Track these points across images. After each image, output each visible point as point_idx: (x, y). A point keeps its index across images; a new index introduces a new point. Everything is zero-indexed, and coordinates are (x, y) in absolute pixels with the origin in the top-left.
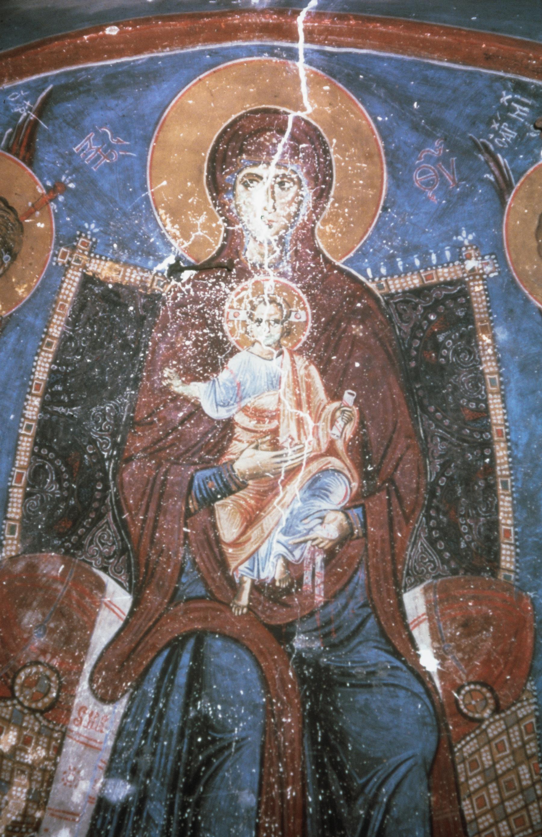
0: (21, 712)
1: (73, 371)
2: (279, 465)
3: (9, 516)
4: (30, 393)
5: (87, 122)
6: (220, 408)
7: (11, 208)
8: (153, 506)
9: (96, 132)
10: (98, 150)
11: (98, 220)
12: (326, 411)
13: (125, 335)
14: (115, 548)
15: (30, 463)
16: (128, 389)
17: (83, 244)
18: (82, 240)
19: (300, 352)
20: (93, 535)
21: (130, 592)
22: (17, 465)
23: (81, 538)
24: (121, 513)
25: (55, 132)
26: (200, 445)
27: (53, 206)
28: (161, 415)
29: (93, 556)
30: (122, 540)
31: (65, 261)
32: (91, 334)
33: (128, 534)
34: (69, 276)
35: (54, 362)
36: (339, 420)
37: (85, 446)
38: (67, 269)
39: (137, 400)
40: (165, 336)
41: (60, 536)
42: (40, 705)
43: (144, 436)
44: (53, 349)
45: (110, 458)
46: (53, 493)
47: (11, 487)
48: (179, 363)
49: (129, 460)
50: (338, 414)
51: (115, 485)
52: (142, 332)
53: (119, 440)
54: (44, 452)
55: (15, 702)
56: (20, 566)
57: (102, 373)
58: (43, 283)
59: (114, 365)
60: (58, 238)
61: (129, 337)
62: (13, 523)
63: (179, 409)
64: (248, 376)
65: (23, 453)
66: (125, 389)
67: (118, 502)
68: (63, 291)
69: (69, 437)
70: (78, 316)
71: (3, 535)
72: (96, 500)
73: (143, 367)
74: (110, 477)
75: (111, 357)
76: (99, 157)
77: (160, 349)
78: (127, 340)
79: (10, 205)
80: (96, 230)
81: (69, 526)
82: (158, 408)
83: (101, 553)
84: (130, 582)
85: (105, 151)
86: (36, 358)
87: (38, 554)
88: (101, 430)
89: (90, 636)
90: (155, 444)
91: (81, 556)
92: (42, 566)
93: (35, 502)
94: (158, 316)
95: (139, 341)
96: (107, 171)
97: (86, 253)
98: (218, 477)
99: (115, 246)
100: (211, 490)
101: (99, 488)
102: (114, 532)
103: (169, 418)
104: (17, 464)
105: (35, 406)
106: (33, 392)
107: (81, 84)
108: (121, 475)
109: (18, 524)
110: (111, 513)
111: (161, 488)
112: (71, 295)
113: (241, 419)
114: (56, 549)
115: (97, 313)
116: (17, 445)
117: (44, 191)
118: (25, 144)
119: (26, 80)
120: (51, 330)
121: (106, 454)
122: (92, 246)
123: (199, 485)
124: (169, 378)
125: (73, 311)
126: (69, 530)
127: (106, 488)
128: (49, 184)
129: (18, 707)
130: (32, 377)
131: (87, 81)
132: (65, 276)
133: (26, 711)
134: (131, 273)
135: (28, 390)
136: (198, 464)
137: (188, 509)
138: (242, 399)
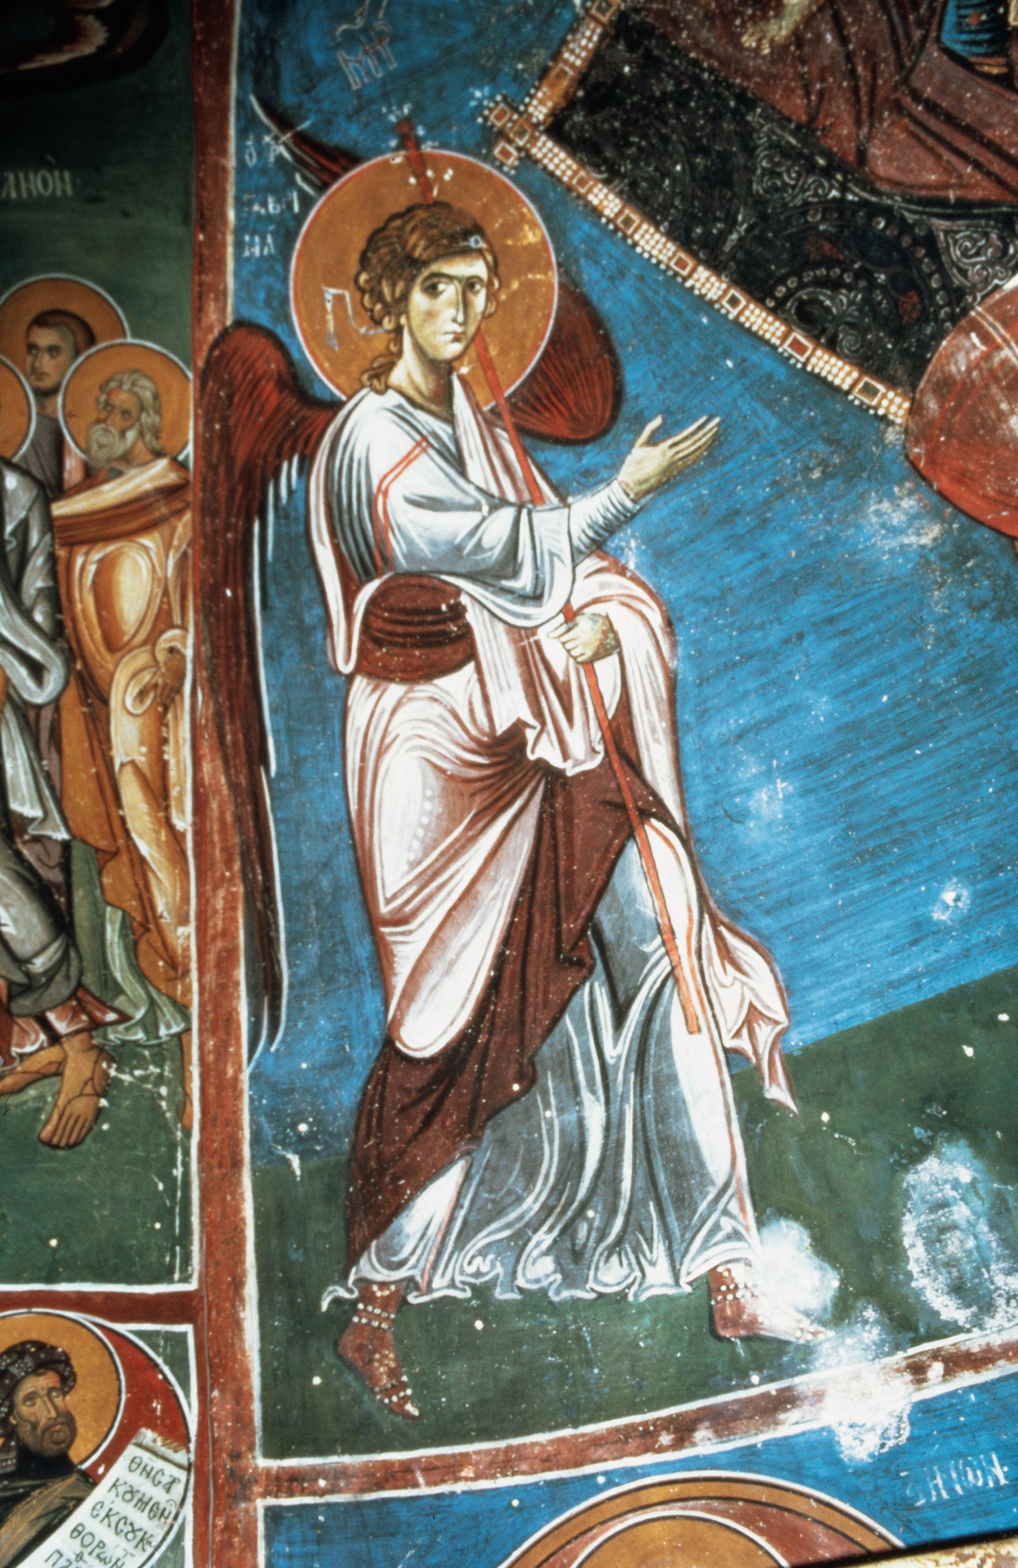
1: (684, 199)
3: (845, 387)
4: (685, 279)
5: (319, 58)
7: (410, 210)
8: (963, 143)
9: (339, 46)
10: (366, 52)
13: (664, 93)
14: (994, 236)
15: (785, 321)
16: (749, 118)
17: (498, 117)
18: (492, 118)
20: (954, 264)
22: (778, 342)
23: (946, 285)
24: (943, 203)
25: (320, 111)
26: (896, 19)
27: (427, 148)
28: (816, 73)
29: (986, 281)
30: (988, 217)
31: (515, 153)
32: (640, 149)
33: (985, 203)
34: (539, 155)
35: (657, 225)
37: (806, 222)
38: (529, 156)
39: (773, 108)
40: (688, 26)
41: (924, 318)
43: (837, 117)
44: (636, 218)
45: (844, 189)
46: (851, 303)
47: (805, 365)
48: (741, 14)
49: (862, 156)
51: (890, 196)
52: (671, 64)
53: (821, 162)
54: (781, 291)
56: (932, 405)
57: (706, 151)
58: (535, 198)
59: (702, 128)
60: (478, 155)
61: (670, 88)
62: (861, 385)
63: (819, 38)
65: (766, 326)
66: (748, 123)
67: (923, 202)
68: (558, 173)
69: (779, 243)
70: (605, 161)
71: (869, 407)
72: (898, 238)
73: (726, 80)
74: (874, 199)
75: (690, 129)
76: (378, 54)
77: (707, 41)
78: (673, 93)
79: (403, 209)
80: (487, 90)
81: (915, 299)
82: (802, 76)
83: (990, 263)
85: (370, 40)
86: (639, 250)
87: (930, 368)
88: (794, 187)
90: (858, 101)
92: (953, 368)
93: (847, 339)
94: (653, 28)
95: (683, 74)
96: (401, 46)
97: (515, 117)
99: (520, 66)
100: (983, 23)
101: (882, 225)
102: (968, 227)
103: (827, 62)
104: (776, 341)
105: (708, 280)
106: (685, 273)
107: (260, 50)
109: (866, 379)
110: (935, 221)
111: (937, 116)
112: (569, 162)
114: (939, 335)
115: (614, 130)
116: (749, 330)
117: (402, 153)
118: (325, 163)
119: (232, 132)
120: (607, 212)
121: (834, 193)
122: (509, 105)
123: (965, 43)
124: (759, 41)
125: (596, 167)
126: (922, 301)
127: (887, 212)
128: (393, 143)
130: (663, 267)
131: (259, 40)
132: (537, 162)
134: (572, 52)
136: (928, 32)
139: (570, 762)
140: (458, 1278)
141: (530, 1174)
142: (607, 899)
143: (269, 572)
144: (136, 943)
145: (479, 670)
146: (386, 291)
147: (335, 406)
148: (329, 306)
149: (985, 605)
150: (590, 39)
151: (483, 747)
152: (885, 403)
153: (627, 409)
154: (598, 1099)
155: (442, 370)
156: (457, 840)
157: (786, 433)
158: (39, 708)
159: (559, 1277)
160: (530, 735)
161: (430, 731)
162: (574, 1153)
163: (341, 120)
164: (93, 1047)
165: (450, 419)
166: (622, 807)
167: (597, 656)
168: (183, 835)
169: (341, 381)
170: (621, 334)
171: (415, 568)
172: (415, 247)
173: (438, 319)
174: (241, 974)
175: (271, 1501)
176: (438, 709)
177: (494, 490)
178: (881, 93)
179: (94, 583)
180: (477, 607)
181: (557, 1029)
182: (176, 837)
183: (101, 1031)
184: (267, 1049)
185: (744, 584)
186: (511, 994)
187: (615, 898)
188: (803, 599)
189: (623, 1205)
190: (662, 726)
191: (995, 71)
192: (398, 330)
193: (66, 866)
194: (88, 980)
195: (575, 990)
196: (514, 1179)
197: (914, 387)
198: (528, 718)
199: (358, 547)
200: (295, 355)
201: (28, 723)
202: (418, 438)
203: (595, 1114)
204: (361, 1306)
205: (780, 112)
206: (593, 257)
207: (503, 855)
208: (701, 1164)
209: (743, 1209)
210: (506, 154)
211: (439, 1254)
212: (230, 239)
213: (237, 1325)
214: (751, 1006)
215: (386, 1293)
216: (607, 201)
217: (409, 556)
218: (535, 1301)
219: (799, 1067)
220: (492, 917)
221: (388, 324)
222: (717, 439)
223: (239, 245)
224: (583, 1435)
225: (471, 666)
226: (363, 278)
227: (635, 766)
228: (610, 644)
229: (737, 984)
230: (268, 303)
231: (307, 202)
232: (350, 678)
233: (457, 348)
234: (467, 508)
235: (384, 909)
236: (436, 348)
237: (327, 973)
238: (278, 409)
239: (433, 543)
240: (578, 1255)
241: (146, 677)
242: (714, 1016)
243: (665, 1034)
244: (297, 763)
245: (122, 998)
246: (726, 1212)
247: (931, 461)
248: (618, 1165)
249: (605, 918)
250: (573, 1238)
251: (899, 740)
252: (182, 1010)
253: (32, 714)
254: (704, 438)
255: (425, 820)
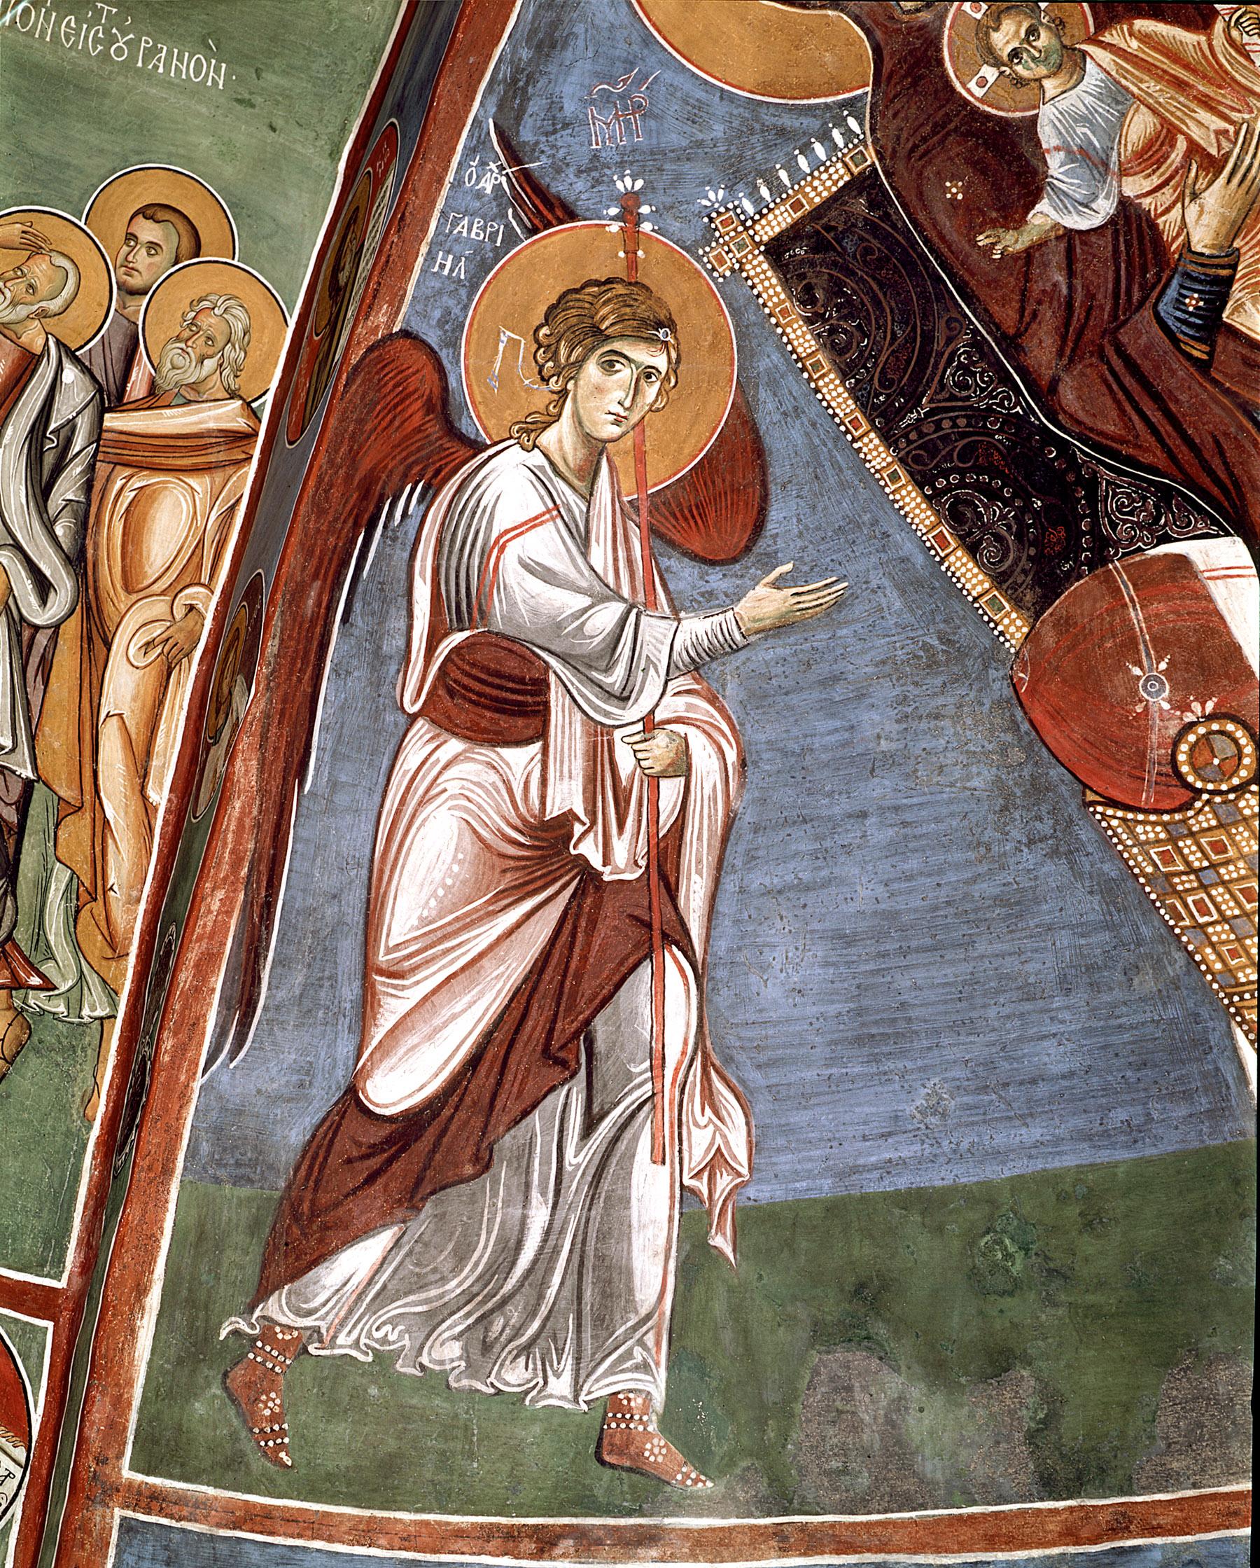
0: (1224, 802)
2: (1247, 182)
4: (854, 440)
5: (570, 107)
6: (1094, 206)
7: (609, 281)
9: (593, 102)
10: (617, 117)
11: (709, 183)
12: (1218, 50)
15: (937, 513)
19: (1101, 27)
21: (1228, 534)
27: (646, 227)
29: (1131, 540)
35: (844, 376)
36: (1246, 38)
42: (1243, 773)
44: (827, 366)
46: (1003, 517)
50: (1235, 33)
54: (941, 483)
55: (1205, 797)
64: (1079, 130)
76: (628, 122)
84: (1215, 522)
88: (983, 390)
89: (1229, 633)
91: (1116, 553)
93: (989, 550)
96: (652, 124)
97: (740, 229)
98: (1188, 284)
106: (856, 434)
107: (515, 81)
108: (1065, 412)
113: (1133, 186)
118: (541, 207)
119: (460, 147)
127: (1063, 446)
128: (614, 211)
129: (1218, 799)
131: (517, 70)
133: (1232, 796)
135: (849, 437)
137: (1195, 361)
138: (1106, 165)
139: (608, 869)
140: (363, 1340)
141: (461, 1256)
142: (608, 1010)
143: (360, 588)
144: (78, 912)
145: (545, 751)
146: (563, 352)
147: (477, 447)
148: (501, 347)
149: (1043, 839)
150: (835, 183)
151: (527, 828)
152: (1006, 621)
153: (762, 545)
154: (546, 1202)
155: (595, 449)
156: (476, 910)
157: (908, 618)
158: (37, 628)
159: (463, 1364)
160: (578, 829)
161: (479, 796)
162: (510, 1247)
163: (571, 170)
164: (10, 1007)
165: (588, 497)
166: (649, 926)
167: (664, 775)
168: (156, 809)
169: (490, 424)
170: (778, 470)
171: (510, 632)
172: (604, 318)
173: (606, 394)
174: (218, 982)
175: (129, 1513)
176: (494, 777)
177: (611, 580)
178: (1089, 335)
179: (127, 510)
180: (561, 688)
181: (524, 1123)
182: (148, 809)
183: (23, 991)
184: (225, 1065)
185: (825, 748)
186: (487, 1077)
187: (616, 1012)
188: (876, 780)
189: (544, 1311)
190: (708, 861)
191: (1196, 353)
192: (563, 393)
193: (23, 806)
194: (19, 935)
195: (552, 1089)
196: (444, 1259)
197: (1037, 615)
198: (580, 811)
199: (458, 592)
200: (452, 382)
201: (20, 642)
202: (551, 505)
203: (539, 1216)
204: (259, 1344)
205: (991, 316)
206: (773, 385)
207: (516, 940)
208: (630, 1291)
209: (658, 1344)
210: (722, 262)
211: (351, 1312)
212: (424, 249)
213: (133, 1331)
214: (719, 1149)
215: (288, 1337)
216: (803, 339)
217: (507, 619)
218: (434, 1381)
219: (751, 1221)
220: (489, 997)
221: (554, 384)
222: (839, 604)
223: (431, 257)
224: (448, 1524)
225: (538, 746)
226: (545, 331)
227: (672, 892)
228: (682, 766)
229: (711, 1127)
230: (442, 323)
231: (511, 239)
232: (413, 718)
233: (616, 431)
234: (578, 590)
235: (382, 958)
236: (595, 423)
237: (306, 1006)
238: (418, 430)
239: (535, 612)
240: (486, 1347)
241: (157, 630)
242: (680, 1151)
243: (631, 1155)
244: (334, 785)
245: (51, 964)
246: (641, 1342)
247: (1032, 690)
248: (550, 1271)
249: (601, 1026)
250: (487, 1330)
251: (928, 941)
252: (112, 994)
253: (26, 634)
254: (828, 597)
255: (449, 882)
